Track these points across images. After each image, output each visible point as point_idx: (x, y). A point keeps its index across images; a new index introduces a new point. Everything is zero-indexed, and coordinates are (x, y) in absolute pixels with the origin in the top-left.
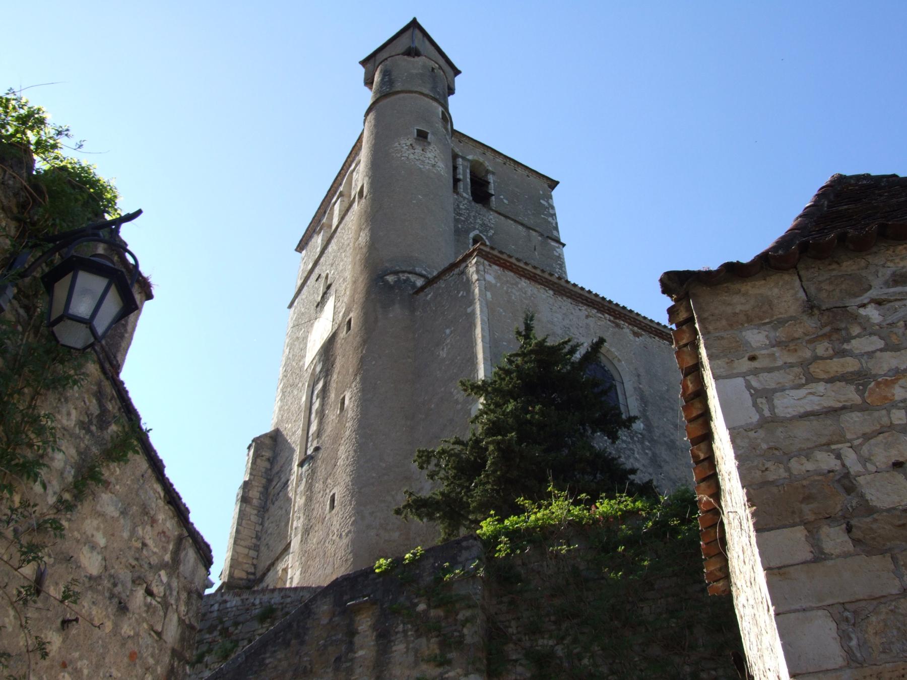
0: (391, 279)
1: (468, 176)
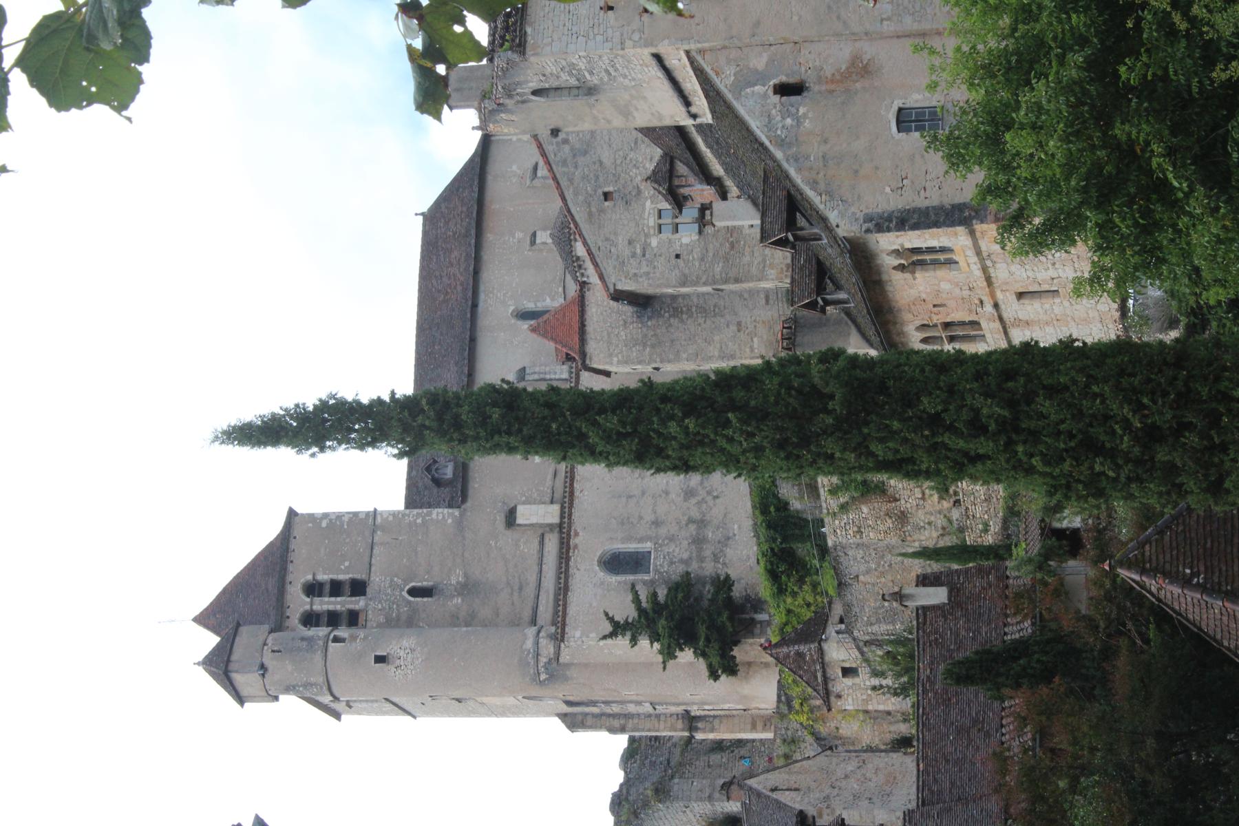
0: (543, 677)
1: (333, 599)
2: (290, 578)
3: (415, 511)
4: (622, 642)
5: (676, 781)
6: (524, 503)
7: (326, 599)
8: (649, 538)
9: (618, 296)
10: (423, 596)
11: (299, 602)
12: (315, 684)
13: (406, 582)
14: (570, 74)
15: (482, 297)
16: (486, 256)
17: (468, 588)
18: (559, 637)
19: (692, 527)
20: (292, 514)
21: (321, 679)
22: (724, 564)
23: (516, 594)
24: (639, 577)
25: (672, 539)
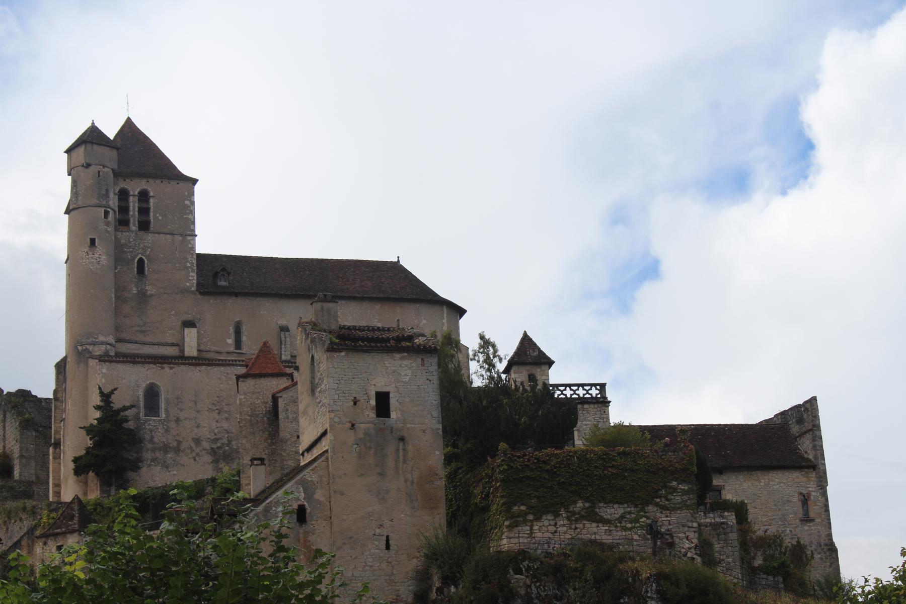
0: (80, 348)
1: (137, 209)
2: (151, 181)
3: (195, 262)
4: (96, 400)
5: (34, 434)
6: (198, 332)
7: (137, 205)
8: (168, 415)
9: (275, 399)
10: (138, 268)
11: (135, 187)
12: (77, 200)
13: (148, 257)
14: (320, 379)
16: (365, 304)
17: (143, 297)
18: (104, 359)
19: (175, 444)
20: (194, 181)
21: (80, 203)
22: (150, 465)
23: (138, 328)
24: (142, 410)
25: (167, 431)
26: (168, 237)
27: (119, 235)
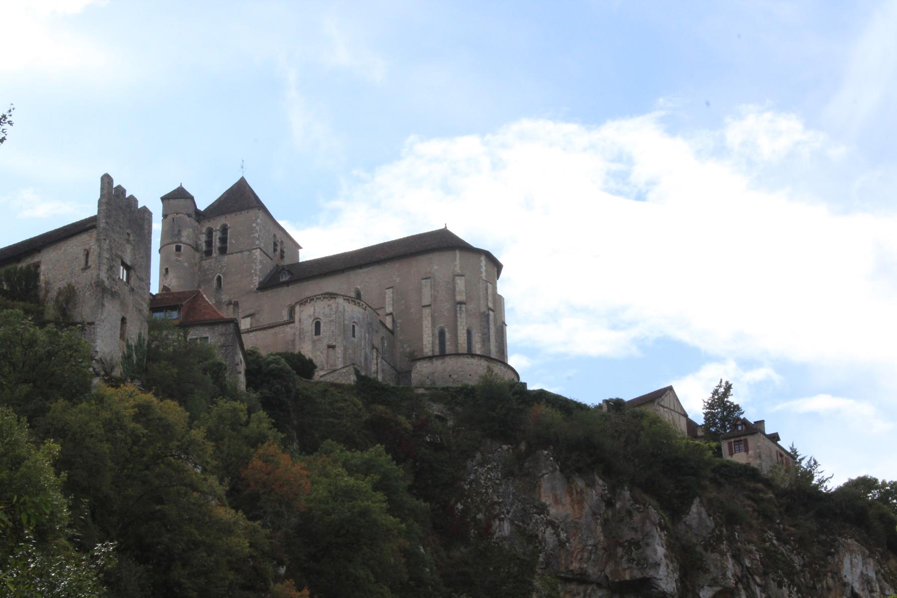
2: (228, 216)
13: (224, 274)
15: (366, 270)
26: (239, 254)
27: (204, 263)
